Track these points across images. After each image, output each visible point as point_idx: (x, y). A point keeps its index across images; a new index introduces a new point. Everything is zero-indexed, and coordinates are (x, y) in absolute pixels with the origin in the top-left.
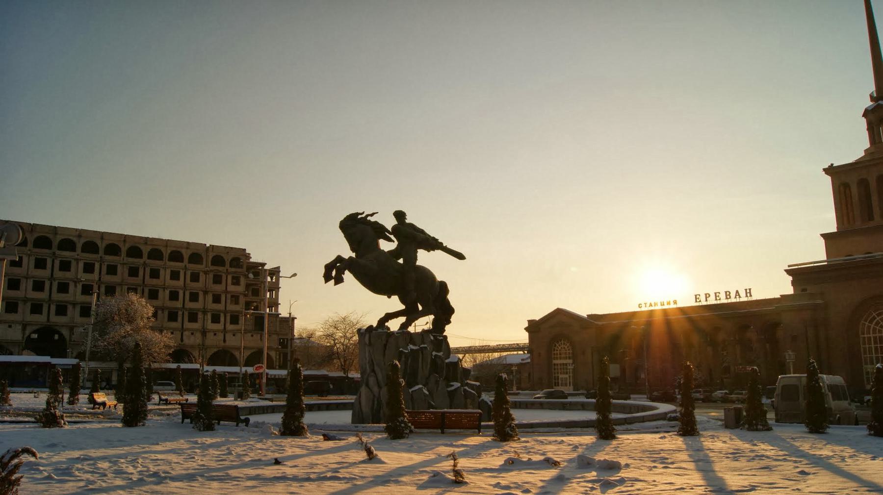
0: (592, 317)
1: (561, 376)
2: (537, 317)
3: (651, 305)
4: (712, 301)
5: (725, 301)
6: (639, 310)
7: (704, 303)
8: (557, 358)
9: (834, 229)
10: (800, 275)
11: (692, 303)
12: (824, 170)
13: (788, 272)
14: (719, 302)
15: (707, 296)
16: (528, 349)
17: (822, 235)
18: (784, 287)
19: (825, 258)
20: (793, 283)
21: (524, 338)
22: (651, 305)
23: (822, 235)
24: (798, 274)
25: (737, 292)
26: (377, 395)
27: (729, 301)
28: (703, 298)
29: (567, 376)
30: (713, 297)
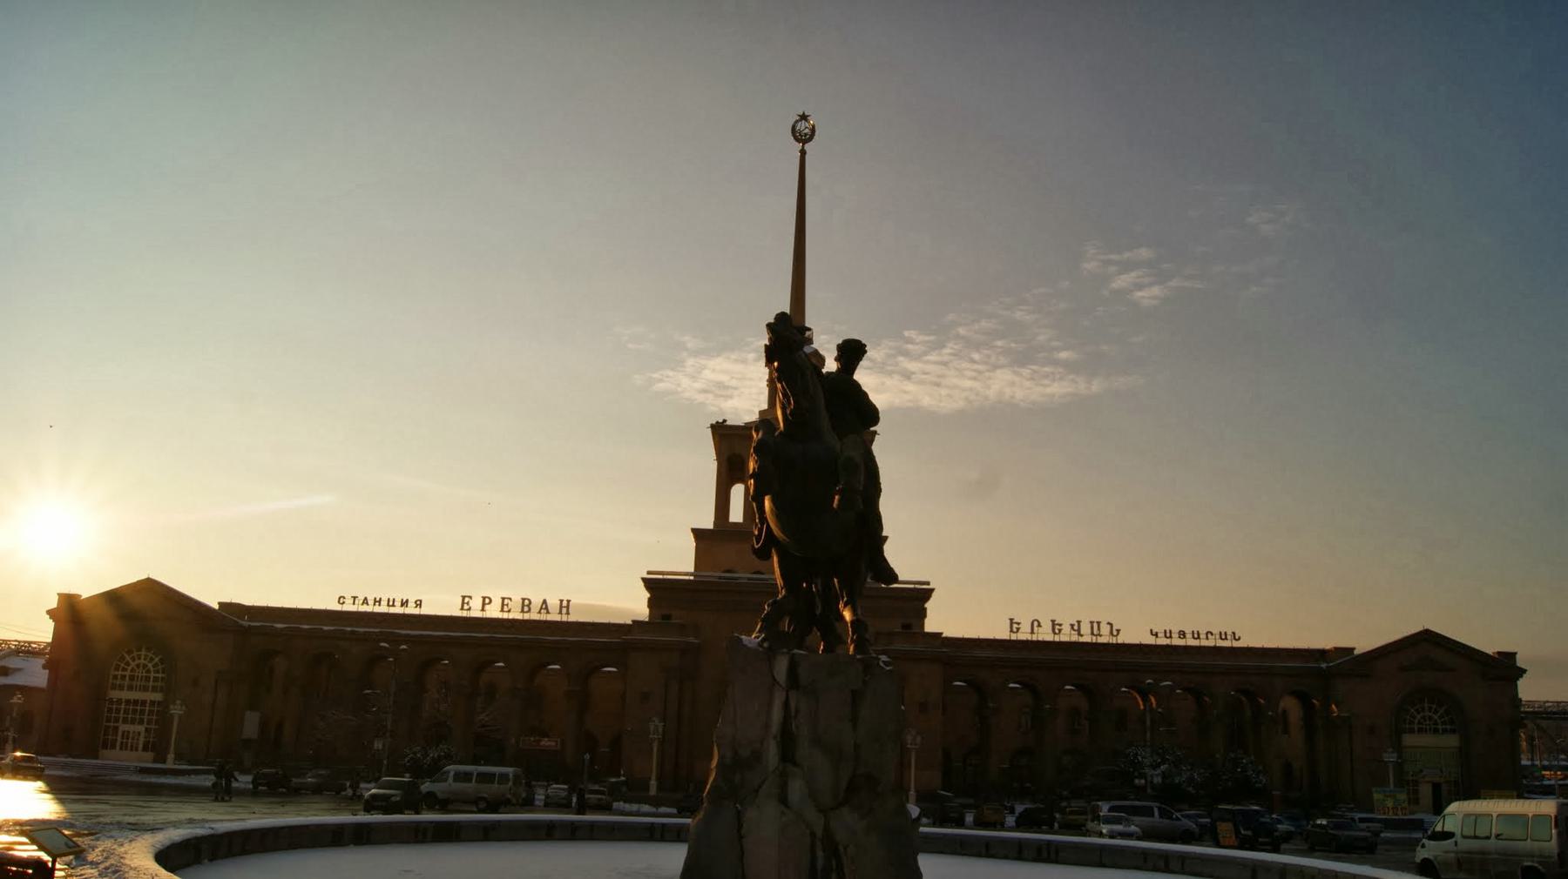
0: (231, 610)
1: (123, 727)
2: (88, 588)
3: (365, 601)
4: (493, 612)
5: (519, 616)
6: (338, 608)
7: (476, 613)
8: (121, 688)
9: (710, 526)
10: (657, 587)
11: (451, 609)
12: (712, 426)
13: (649, 584)
14: (505, 616)
15: (486, 601)
16: (53, 656)
17: (694, 531)
18: (634, 605)
19: (692, 570)
20: (652, 603)
21: (42, 632)
22: (365, 601)
23: (694, 531)
24: (657, 587)
25: (545, 602)
26: (819, 833)
27: (527, 616)
28: (476, 604)
29: (141, 728)
30: (497, 603)
